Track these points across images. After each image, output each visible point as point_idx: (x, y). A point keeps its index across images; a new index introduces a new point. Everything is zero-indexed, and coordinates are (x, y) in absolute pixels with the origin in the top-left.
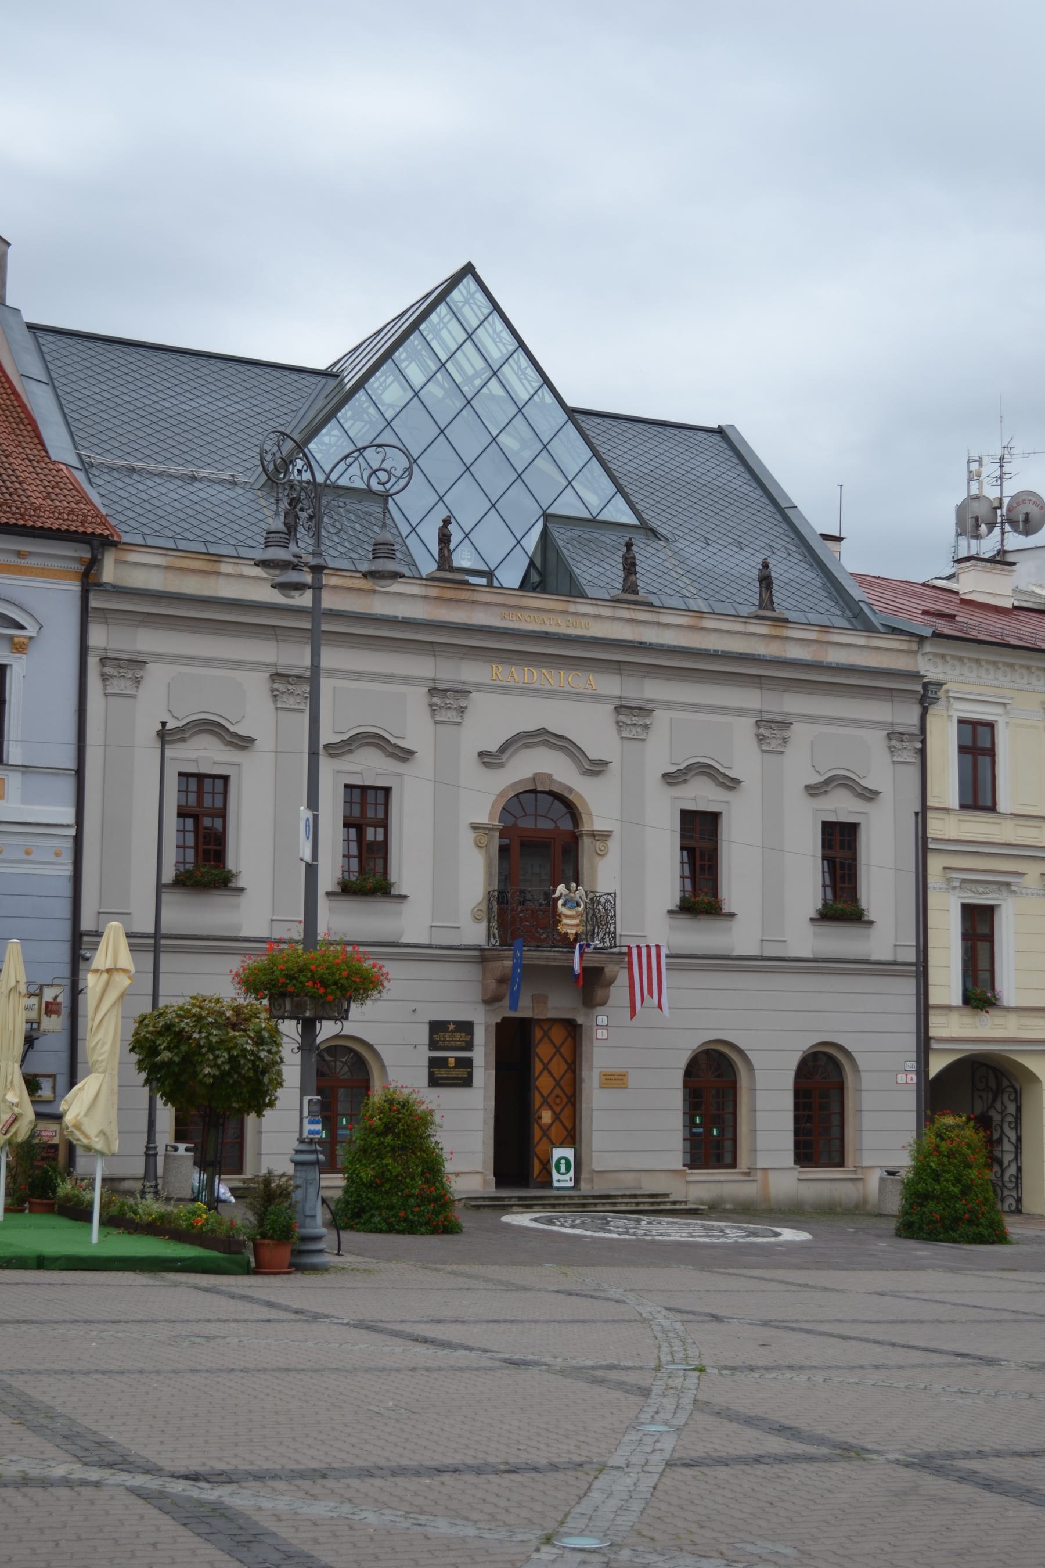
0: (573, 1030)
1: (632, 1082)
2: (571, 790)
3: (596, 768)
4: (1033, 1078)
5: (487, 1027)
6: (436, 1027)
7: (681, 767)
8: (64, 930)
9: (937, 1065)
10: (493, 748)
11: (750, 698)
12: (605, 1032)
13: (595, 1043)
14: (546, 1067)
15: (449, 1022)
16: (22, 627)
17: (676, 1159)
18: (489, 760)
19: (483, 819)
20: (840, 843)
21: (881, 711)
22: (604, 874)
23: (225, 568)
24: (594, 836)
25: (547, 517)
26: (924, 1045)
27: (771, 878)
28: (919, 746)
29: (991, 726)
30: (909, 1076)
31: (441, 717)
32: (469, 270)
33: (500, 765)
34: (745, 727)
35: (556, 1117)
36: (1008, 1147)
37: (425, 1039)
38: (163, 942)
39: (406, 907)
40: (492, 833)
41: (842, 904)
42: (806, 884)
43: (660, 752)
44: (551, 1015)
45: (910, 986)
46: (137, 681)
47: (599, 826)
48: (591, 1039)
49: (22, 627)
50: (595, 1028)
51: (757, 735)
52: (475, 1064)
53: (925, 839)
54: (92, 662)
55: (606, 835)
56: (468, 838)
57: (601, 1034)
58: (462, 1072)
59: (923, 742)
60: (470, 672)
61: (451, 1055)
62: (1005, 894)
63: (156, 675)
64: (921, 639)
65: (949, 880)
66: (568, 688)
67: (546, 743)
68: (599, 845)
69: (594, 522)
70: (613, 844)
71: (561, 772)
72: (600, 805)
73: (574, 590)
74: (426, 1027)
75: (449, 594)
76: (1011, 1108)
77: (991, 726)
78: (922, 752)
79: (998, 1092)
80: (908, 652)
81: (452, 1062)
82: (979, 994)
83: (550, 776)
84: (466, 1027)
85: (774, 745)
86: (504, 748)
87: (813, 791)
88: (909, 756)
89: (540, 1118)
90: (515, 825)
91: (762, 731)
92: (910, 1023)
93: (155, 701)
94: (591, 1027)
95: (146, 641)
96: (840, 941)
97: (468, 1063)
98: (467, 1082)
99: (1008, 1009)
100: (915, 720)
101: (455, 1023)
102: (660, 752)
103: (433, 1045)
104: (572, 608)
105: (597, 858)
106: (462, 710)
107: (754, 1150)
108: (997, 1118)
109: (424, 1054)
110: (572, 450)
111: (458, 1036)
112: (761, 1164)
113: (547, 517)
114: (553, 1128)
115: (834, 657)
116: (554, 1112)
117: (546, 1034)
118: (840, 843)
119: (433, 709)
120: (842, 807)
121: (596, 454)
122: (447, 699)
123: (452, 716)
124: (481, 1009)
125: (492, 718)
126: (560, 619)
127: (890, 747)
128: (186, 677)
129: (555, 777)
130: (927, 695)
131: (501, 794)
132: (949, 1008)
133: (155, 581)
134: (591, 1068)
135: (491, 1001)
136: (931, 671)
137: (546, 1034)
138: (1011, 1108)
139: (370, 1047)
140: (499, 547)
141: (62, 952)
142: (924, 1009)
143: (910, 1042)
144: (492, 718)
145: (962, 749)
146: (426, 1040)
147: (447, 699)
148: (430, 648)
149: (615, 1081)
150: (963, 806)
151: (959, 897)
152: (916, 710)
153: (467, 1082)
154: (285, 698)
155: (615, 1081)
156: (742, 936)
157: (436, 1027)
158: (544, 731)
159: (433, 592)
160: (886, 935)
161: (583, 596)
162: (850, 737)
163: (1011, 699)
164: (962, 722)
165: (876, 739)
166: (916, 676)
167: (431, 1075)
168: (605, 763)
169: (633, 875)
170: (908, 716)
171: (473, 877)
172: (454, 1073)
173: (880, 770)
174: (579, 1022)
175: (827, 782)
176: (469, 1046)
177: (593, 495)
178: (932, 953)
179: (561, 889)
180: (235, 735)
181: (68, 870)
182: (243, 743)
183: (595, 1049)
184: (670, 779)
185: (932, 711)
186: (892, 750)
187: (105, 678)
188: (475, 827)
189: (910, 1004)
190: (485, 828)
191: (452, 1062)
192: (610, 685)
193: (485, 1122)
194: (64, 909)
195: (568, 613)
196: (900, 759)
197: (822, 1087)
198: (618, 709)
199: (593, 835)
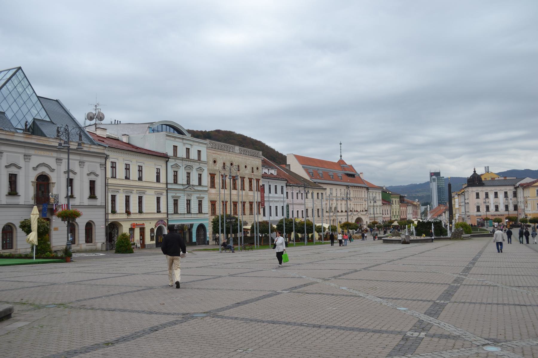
4: (121, 225)
10: (35, 166)
18: (34, 169)
20: (92, 184)
21: (99, 160)
22: (54, 191)
25: (34, 119)
26: (106, 220)
36: (115, 237)
39: (20, 197)
41: (93, 196)
45: (104, 210)
47: (53, 181)
55: (55, 183)
56: (31, 184)
57: (54, 220)
60: (31, 152)
64: (106, 147)
69: (42, 120)
70: (56, 185)
73: (43, 135)
76: (116, 231)
77: (115, 163)
78: (105, 168)
79: (113, 228)
82: (114, 212)
85: (82, 166)
86: (37, 166)
87: (88, 175)
88: (104, 168)
100: (104, 162)
106: (30, 159)
107: (79, 241)
108: (113, 233)
112: (80, 243)
113: (34, 119)
115: (92, 150)
118: (92, 184)
119: (25, 159)
120: (93, 178)
122: (27, 157)
125: (35, 160)
130: (107, 157)
138: (116, 231)
142: (106, 214)
143: (104, 220)
144: (35, 160)
145: (111, 167)
147: (27, 157)
148: (25, 147)
149: (56, 229)
152: (104, 160)
155: (56, 229)
158: (44, 163)
159: (25, 136)
160: (99, 201)
161: (45, 136)
162: (93, 165)
165: (98, 165)
166: (104, 154)
168: (54, 170)
170: (103, 161)
171: (32, 191)
173: (99, 171)
175: (91, 173)
177: (43, 115)
185: (107, 160)
188: (32, 182)
189: (104, 213)
198: (57, 159)
199: (52, 183)
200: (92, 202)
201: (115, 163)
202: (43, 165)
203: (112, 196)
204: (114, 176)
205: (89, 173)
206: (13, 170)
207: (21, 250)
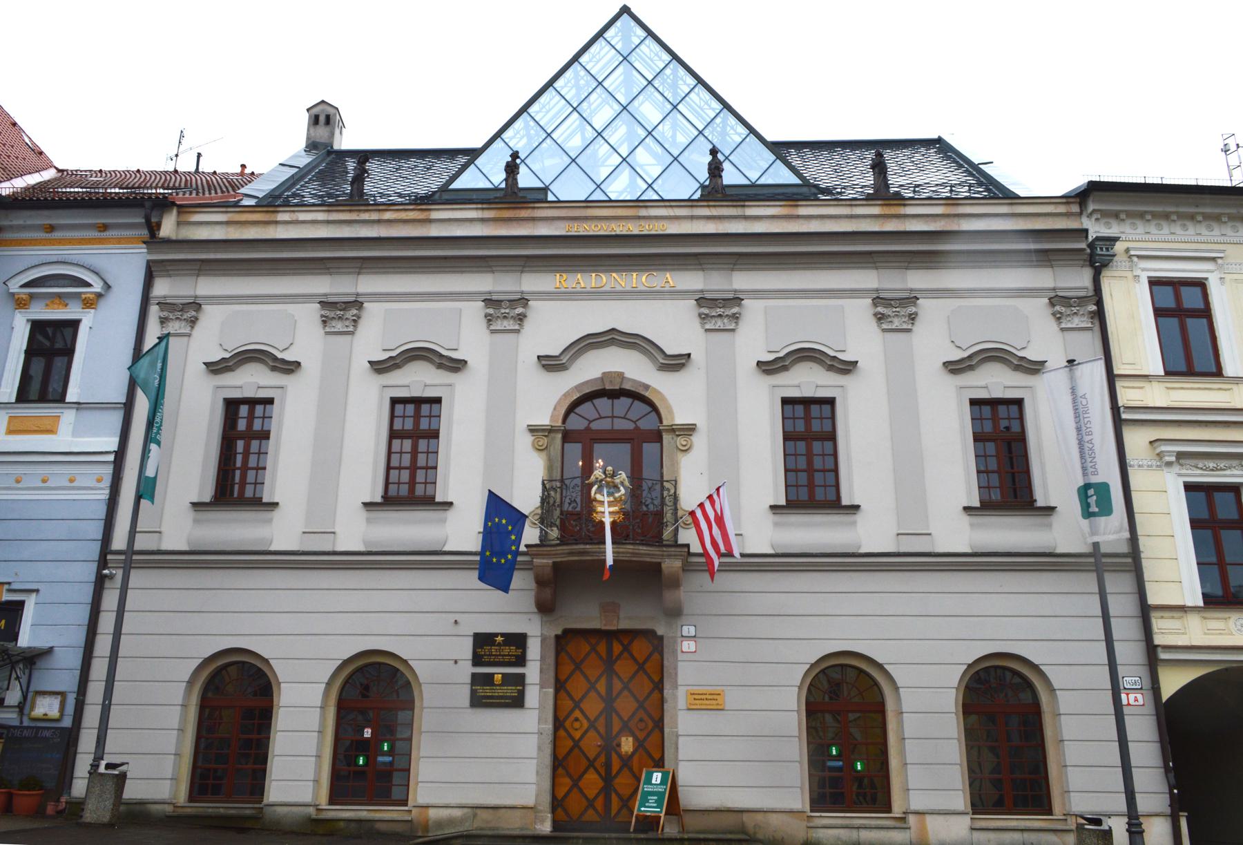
0: (657, 644)
1: (732, 698)
2: (647, 387)
3: (677, 363)
5: (543, 641)
6: (482, 641)
7: (781, 354)
8: (94, 550)
9: (1172, 682)
12: (692, 644)
13: (680, 657)
15: (496, 635)
16: (89, 285)
17: (798, 799)
18: (550, 364)
19: (544, 420)
24: (673, 431)
28: (1094, 308)
30: (1132, 697)
31: (498, 325)
34: (862, 308)
35: (639, 745)
37: (468, 654)
38: (135, 557)
40: (552, 435)
44: (624, 625)
47: (680, 419)
48: (674, 652)
49: (89, 285)
50: (679, 640)
51: (875, 315)
52: (528, 681)
54: (154, 310)
55: (690, 429)
56: (525, 441)
57: (688, 646)
58: (511, 691)
59: (1100, 303)
63: (212, 316)
65: (1160, 455)
66: (641, 288)
68: (681, 441)
70: (698, 440)
71: (634, 368)
72: (680, 399)
74: (471, 640)
77: (1201, 284)
78: (1100, 315)
81: (498, 678)
83: (622, 374)
84: (518, 641)
89: (619, 745)
90: (588, 429)
91: (880, 309)
93: (211, 337)
94: (674, 638)
95: (206, 286)
97: (520, 680)
98: (517, 702)
101: (503, 635)
103: (477, 660)
105: (680, 455)
106: (521, 318)
109: (467, 670)
111: (506, 650)
114: (637, 755)
116: (636, 739)
117: (626, 649)
119: (489, 319)
127: (1054, 314)
129: (628, 375)
131: (566, 395)
133: (218, 234)
134: (675, 686)
135: (545, 608)
137: (626, 649)
141: (88, 572)
146: (470, 656)
149: (707, 701)
150: (1168, 373)
151: (1180, 475)
153: (517, 702)
154: (334, 323)
155: (707, 701)
156: (873, 531)
157: (482, 641)
163: (1223, 251)
164: (1154, 283)
167: (473, 692)
169: (728, 469)
170: (1078, 279)
172: (499, 691)
174: (660, 633)
176: (521, 661)
180: (283, 361)
181: (104, 494)
183: (680, 664)
184: (768, 368)
186: (1058, 317)
187: (163, 321)
188: (533, 430)
190: (543, 430)
191: (498, 678)
193: (540, 749)
194: (96, 531)
195: (639, 218)
196: (1069, 326)
197: (1004, 712)
199: (673, 430)
200: (1009, 533)
201: (1201, 284)
202: (612, 338)
204: (1205, 363)
205: (957, 355)
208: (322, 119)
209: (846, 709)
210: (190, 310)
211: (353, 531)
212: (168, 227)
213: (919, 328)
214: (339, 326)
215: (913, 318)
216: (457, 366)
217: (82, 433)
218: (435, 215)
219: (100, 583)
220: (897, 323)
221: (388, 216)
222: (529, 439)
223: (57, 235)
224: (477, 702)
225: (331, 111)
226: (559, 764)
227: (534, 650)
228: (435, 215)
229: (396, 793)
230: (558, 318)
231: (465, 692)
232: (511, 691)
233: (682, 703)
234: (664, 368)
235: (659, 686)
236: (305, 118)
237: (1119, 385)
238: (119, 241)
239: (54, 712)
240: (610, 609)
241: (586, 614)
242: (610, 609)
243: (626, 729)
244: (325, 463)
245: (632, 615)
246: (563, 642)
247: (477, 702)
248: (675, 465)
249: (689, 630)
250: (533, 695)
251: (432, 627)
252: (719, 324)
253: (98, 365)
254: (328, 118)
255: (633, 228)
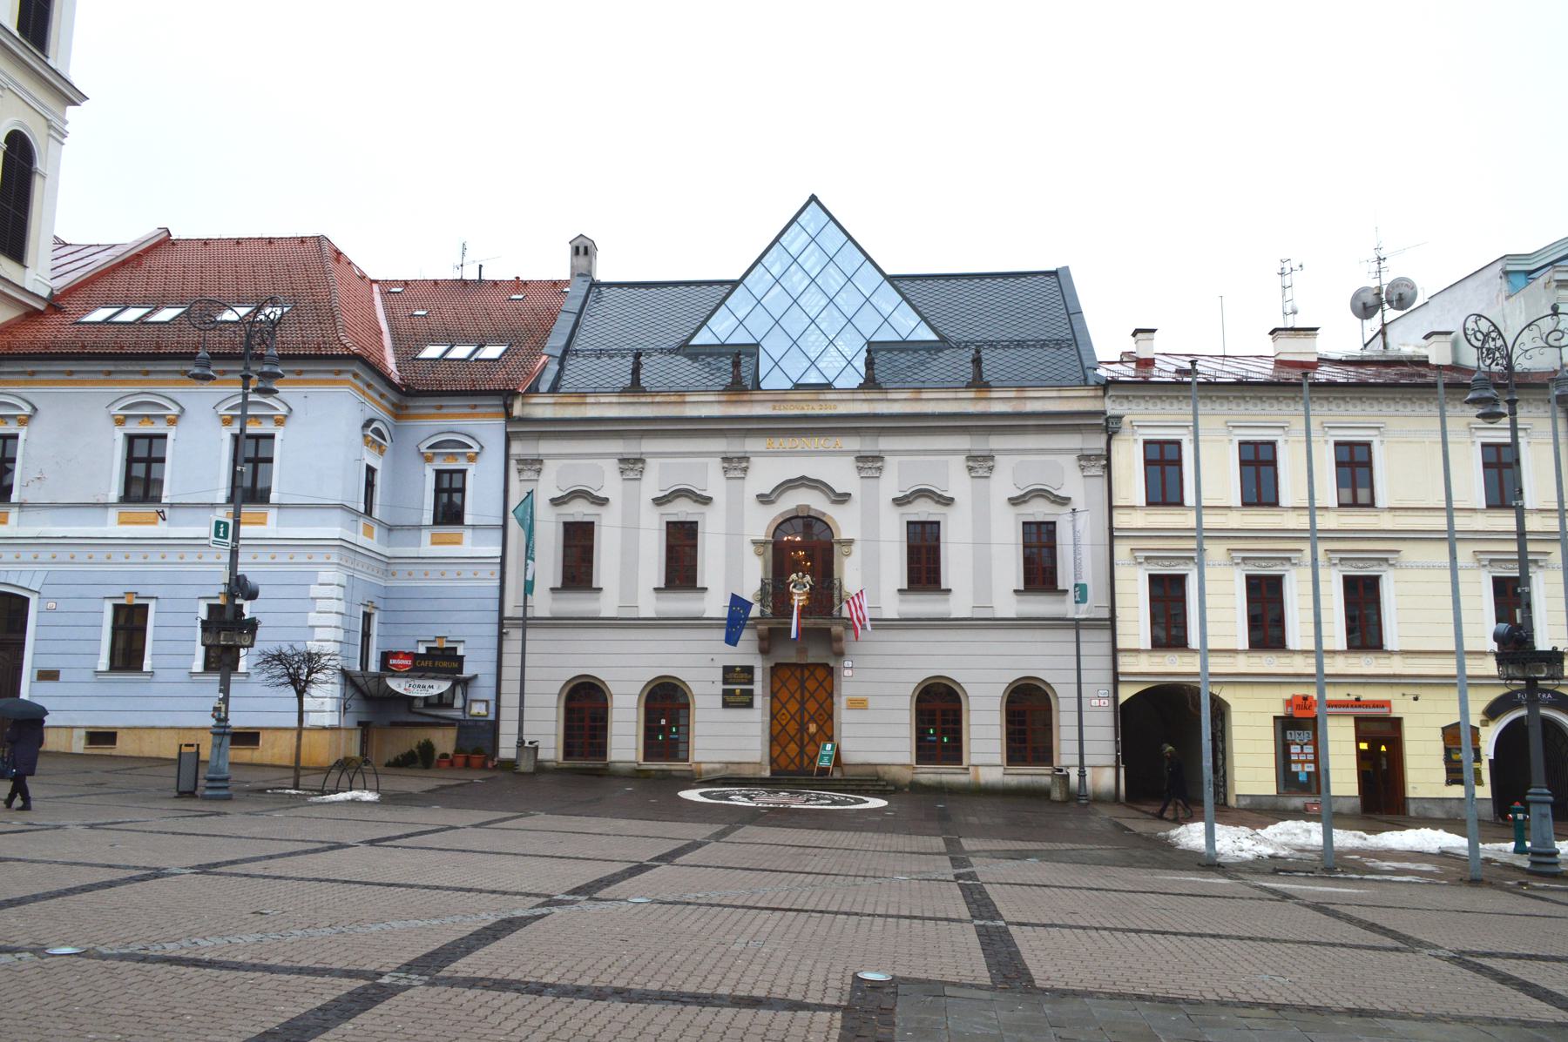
0: (830, 671)
1: (872, 703)
3: (842, 499)
6: (728, 671)
8: (495, 617)
11: (964, 442)
14: (812, 695)
18: (765, 499)
21: (1074, 441)
23: (589, 400)
27: (982, 565)
29: (1368, 445)
31: (731, 474)
32: (813, 198)
33: (772, 502)
35: (820, 728)
42: (653, 565)
43: (893, 481)
44: (810, 660)
45: (1106, 635)
46: (539, 472)
53: (1111, 529)
54: (513, 463)
55: (850, 542)
56: (750, 549)
57: (847, 673)
58: (746, 699)
59: (1109, 459)
61: (738, 687)
62: (1385, 567)
63: (550, 467)
67: (803, 485)
68: (845, 549)
70: (856, 548)
71: (815, 502)
72: (845, 523)
75: (734, 398)
78: (1108, 467)
80: (1095, 397)
83: (808, 507)
84: (749, 670)
92: (1107, 662)
93: (549, 484)
95: (545, 447)
96: (680, 604)
97: (751, 692)
98: (749, 705)
99: (1391, 653)
102: (893, 481)
103: (725, 682)
104: (822, 397)
106: (745, 470)
109: (720, 687)
110: (888, 299)
119: (726, 470)
121: (905, 298)
123: (738, 474)
124: (759, 657)
126: (815, 405)
128: (564, 468)
130: (1110, 428)
132: (1335, 652)
133: (548, 413)
135: (764, 651)
136: (1112, 408)
139: (1048, 685)
140: (841, 365)
141: (494, 629)
149: (858, 704)
153: (749, 705)
155: (858, 704)
156: (959, 604)
157: (728, 671)
158: (803, 478)
162: (1055, 463)
165: (1069, 461)
170: (1097, 443)
176: (751, 682)
178: (1118, 611)
179: (794, 576)
180: (597, 498)
181: (497, 583)
182: (603, 502)
184: (899, 502)
185: (1115, 438)
186: (1083, 468)
187: (520, 471)
188: (754, 543)
192: (853, 444)
194: (495, 605)
197: (1028, 711)
199: (839, 542)
203: (1350, 583)
206: (683, 510)
207: (982, 770)
208: (582, 250)
209: (938, 710)
210: (534, 464)
211: (649, 605)
212: (517, 410)
213: (995, 476)
214: (631, 475)
215: (991, 469)
216: (706, 501)
217: (476, 544)
218: (688, 399)
219: (501, 636)
220: (981, 473)
221: (658, 399)
222: (752, 548)
223: (444, 411)
224: (726, 705)
225: (588, 243)
226: (774, 739)
227: (758, 675)
228: (688, 399)
229: (682, 754)
230: (768, 469)
231: (720, 699)
232: (746, 699)
233: (844, 705)
234: (835, 502)
235: (831, 695)
236: (568, 250)
237: (1115, 513)
238: (485, 415)
239: (483, 712)
240: (802, 651)
241: (789, 656)
242: (802, 651)
243: (812, 719)
244: (629, 562)
245: (814, 655)
246: (776, 671)
247: (726, 705)
248: (841, 564)
249: (848, 664)
250: (758, 701)
251: (699, 663)
252: (870, 473)
253: (480, 499)
254: (586, 252)
255: (817, 411)
